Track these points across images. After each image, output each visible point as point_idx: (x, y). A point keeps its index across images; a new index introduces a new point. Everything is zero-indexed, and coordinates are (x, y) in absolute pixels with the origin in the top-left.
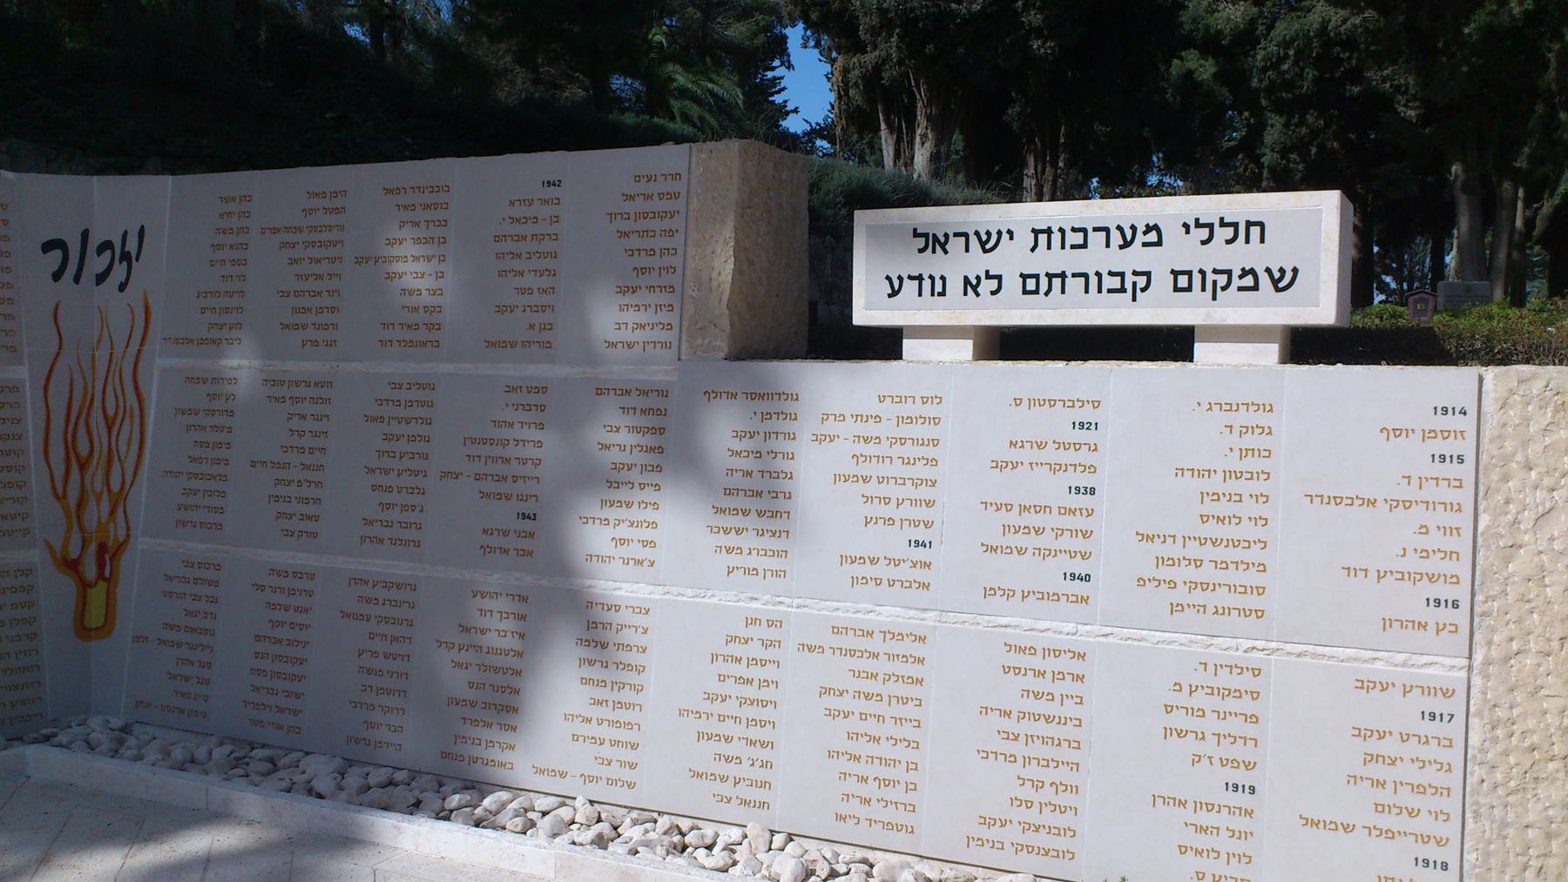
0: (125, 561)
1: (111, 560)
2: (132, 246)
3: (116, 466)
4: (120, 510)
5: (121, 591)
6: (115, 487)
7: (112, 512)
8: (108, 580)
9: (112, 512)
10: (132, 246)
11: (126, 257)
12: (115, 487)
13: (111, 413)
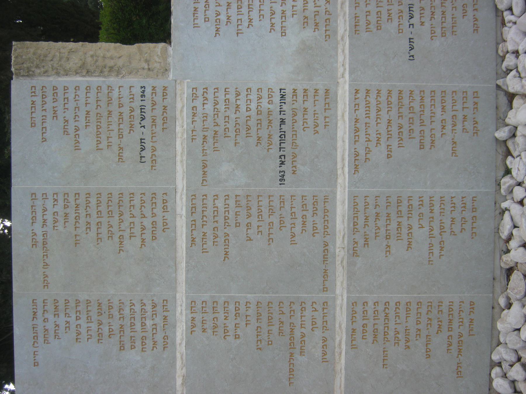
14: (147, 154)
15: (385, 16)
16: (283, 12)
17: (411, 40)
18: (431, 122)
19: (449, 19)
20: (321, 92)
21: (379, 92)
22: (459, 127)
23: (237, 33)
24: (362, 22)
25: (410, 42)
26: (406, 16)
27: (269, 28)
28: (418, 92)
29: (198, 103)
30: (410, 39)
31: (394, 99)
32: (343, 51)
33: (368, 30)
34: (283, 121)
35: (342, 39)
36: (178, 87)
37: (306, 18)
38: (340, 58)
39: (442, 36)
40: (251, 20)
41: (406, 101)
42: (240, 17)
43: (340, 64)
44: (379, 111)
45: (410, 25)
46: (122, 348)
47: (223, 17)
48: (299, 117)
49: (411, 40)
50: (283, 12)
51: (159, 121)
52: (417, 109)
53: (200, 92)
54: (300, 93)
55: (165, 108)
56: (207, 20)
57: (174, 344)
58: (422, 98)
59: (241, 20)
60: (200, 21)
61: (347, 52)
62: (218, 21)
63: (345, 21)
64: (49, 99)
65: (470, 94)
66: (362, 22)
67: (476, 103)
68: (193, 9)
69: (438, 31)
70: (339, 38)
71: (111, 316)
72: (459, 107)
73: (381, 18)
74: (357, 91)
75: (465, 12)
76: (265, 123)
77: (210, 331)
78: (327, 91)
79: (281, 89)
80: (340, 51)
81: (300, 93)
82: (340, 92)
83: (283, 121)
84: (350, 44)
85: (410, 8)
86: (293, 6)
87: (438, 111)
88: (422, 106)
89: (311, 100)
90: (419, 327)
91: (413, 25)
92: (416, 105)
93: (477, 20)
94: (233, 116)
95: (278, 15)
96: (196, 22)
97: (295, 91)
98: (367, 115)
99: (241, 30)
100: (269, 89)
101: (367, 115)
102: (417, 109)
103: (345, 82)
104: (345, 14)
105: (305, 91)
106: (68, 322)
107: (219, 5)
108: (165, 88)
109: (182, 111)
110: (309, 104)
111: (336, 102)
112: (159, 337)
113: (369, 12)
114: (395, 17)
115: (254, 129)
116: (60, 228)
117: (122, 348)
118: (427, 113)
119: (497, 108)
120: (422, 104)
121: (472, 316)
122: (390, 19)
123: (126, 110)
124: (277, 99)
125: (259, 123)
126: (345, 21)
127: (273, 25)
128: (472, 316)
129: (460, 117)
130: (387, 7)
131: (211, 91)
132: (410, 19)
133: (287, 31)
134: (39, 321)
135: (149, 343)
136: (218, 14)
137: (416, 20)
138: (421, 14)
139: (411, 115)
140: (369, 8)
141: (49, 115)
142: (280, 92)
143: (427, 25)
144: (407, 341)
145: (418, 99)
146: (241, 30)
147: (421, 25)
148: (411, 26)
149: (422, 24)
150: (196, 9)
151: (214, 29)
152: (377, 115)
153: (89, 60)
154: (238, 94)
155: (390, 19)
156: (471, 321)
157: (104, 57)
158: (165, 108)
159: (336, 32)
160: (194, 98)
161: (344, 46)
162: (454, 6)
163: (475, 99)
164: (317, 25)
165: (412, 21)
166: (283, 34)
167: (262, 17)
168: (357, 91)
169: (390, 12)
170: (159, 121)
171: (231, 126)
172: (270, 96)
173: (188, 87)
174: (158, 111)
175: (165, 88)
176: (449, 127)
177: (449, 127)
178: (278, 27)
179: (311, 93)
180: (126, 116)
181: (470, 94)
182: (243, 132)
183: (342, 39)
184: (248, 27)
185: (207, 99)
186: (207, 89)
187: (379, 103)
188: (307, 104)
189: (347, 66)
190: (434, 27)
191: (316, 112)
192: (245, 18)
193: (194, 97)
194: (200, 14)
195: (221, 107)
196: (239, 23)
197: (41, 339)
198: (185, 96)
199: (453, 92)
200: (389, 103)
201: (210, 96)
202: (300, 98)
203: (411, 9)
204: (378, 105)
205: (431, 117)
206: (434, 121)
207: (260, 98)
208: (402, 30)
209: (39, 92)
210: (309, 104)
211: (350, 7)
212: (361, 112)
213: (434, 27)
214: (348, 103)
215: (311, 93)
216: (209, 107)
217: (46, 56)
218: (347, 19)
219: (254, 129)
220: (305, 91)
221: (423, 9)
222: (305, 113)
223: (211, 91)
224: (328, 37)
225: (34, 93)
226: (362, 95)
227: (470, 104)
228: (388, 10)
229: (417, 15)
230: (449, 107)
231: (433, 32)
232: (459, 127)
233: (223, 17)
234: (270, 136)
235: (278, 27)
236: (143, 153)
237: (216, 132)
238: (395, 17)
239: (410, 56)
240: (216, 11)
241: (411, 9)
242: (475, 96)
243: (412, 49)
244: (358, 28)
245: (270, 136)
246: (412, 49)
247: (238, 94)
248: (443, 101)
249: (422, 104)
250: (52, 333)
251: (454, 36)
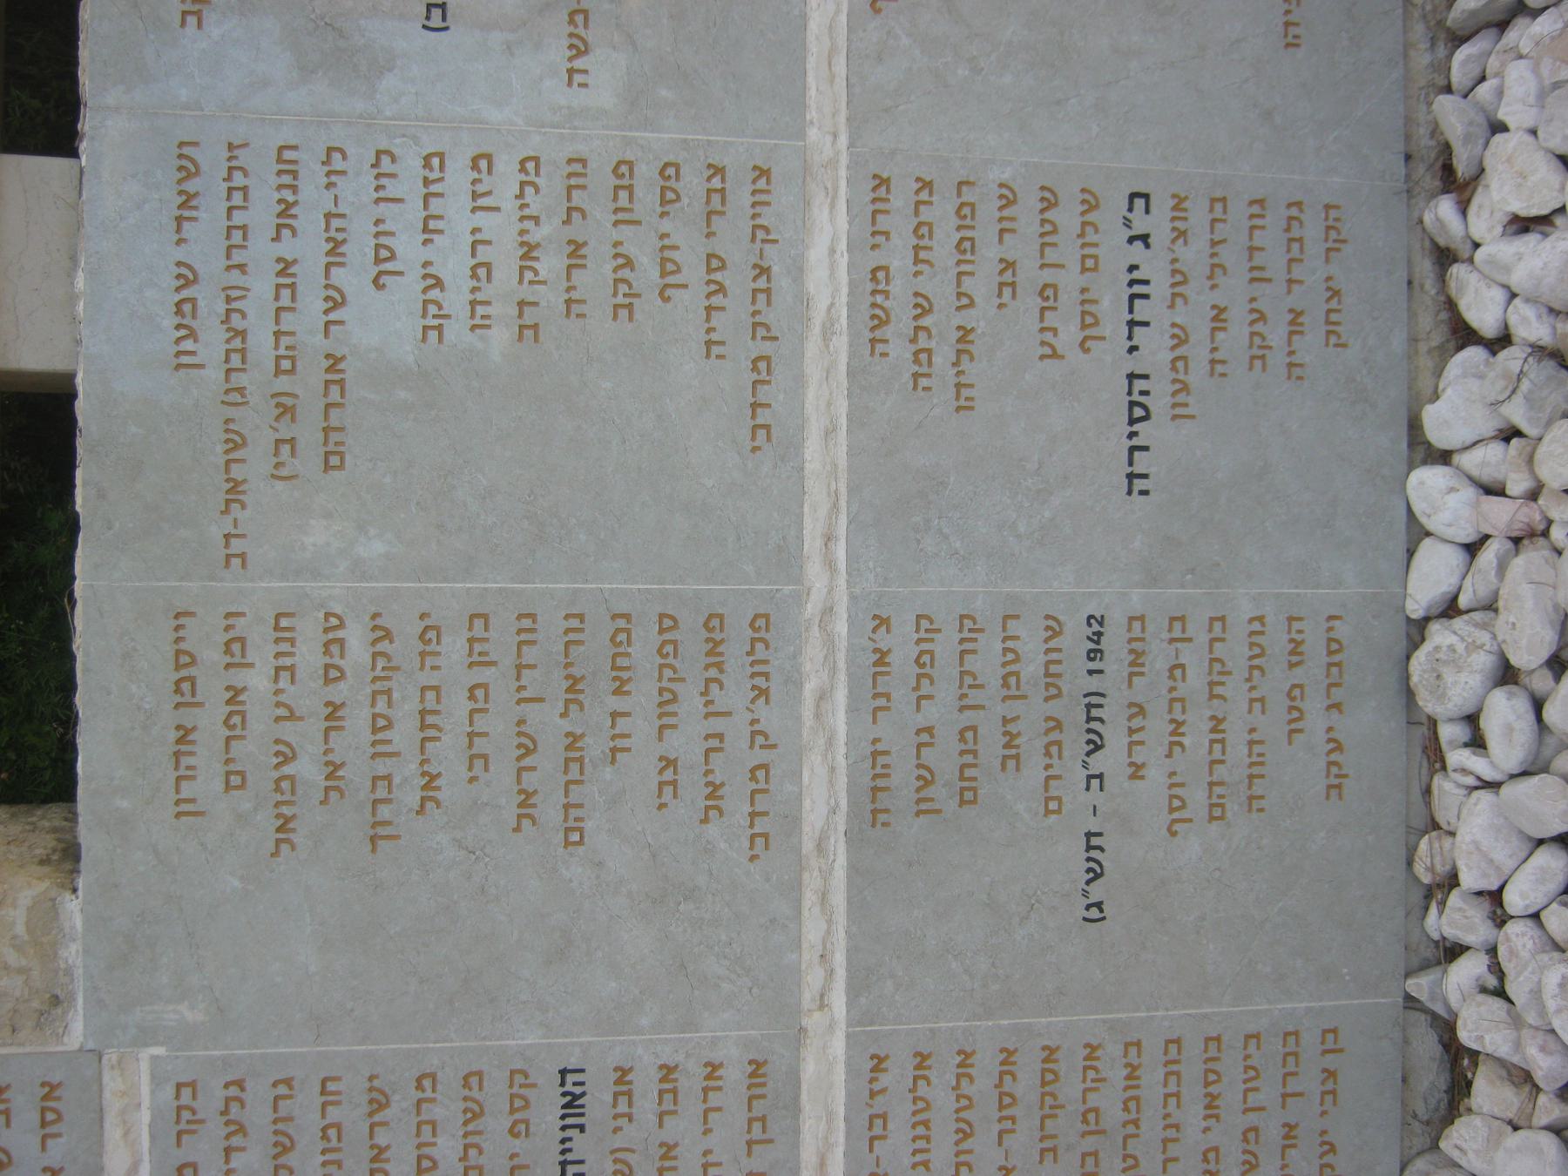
15: (991, 745)
16: (573, 741)
17: (1095, 841)
18: (1166, 1161)
19: (1237, 750)
20: (734, 1075)
21: (966, 1056)
23: (373, 839)
24: (903, 776)
25: (1089, 848)
26: (1075, 742)
27: (510, 814)
28: (1118, 1050)
30: (1089, 835)
31: (1026, 1084)
32: (824, 897)
33: (924, 807)
35: (820, 848)
36: (112, 1082)
37: (669, 763)
38: (813, 930)
39: (1212, 818)
40: (431, 780)
41: (1070, 1088)
42: (382, 768)
43: (809, 956)
44: (965, 1134)
45: (1090, 777)
47: (307, 769)
49: (1095, 841)
50: (573, 741)
52: (1113, 1114)
53: (210, 1102)
54: (646, 1083)
56: (234, 780)
58: (1133, 1073)
59: (388, 778)
60: (207, 784)
61: (839, 899)
62: (285, 786)
63: (833, 769)
65: (1310, 1040)
66: (903, 776)
67: (1330, 1074)
68: (173, 735)
69: (1197, 797)
70: (808, 846)
72: (1267, 1094)
73: (975, 753)
74: (879, 1063)
75: (1296, 714)
78: (757, 1068)
79: (563, 1072)
80: (809, 898)
81: (646, 1083)
82: (809, 1069)
84: (854, 869)
85: (1089, 706)
86: (615, 715)
87: (1192, 1115)
88: (1131, 1102)
89: (691, 1106)
91: (1100, 776)
92: (1109, 1102)
93: (1339, 748)
95: (548, 761)
96: (187, 790)
97: (623, 1074)
98: (918, 1158)
99: (389, 823)
100: (513, 1072)
101: (918, 1158)
102: (1113, 1114)
103: (831, 1027)
104: (830, 742)
105: (668, 1071)
107: (292, 716)
108: (51, 1090)
110: (682, 1128)
111: (794, 1108)
113: (929, 730)
114: (1031, 745)
118: (1152, 1127)
119: (1404, 1080)
120: (1130, 1093)
122: (1012, 757)
126: (833, 769)
127: (527, 799)
129: (1273, 1132)
130: (1001, 709)
131: (259, 1094)
132: (1088, 754)
133: (588, 825)
136: (287, 756)
137: (1110, 760)
138: (1131, 731)
139: (1089, 1143)
140: (931, 713)
142: (563, 1084)
143: (1156, 775)
145: (1118, 1075)
146: (389, 823)
147: (1133, 777)
148: (1095, 783)
150: (185, 735)
151: (266, 822)
152: (957, 1154)
154: (379, 1102)
155: (1012, 757)
159: (793, 821)
160: (183, 1126)
161: (826, 875)
162: (1255, 694)
163: (1329, 1057)
164: (714, 791)
165: (1098, 763)
166: (574, 835)
167: (479, 763)
168: (879, 1063)
169: (1012, 728)
172: (519, 1103)
173: (157, 1081)
175: (51, 1090)
178: (550, 811)
179: (690, 1082)
181: (1310, 1040)
183: (820, 848)
184: (421, 810)
185: (241, 1129)
186: (240, 1084)
187: (965, 1103)
188: (674, 1129)
189: (840, 959)
190: (1182, 785)
191: (711, 1158)
192: (407, 770)
194: (206, 759)
196: (381, 793)
198: (145, 1116)
199: (1248, 1037)
200: (1006, 1100)
201: (258, 1115)
202: (646, 1106)
203: (1095, 712)
204: (962, 1115)
205: (1165, 1141)
206: (1175, 1159)
207: (474, 1113)
208: (1059, 799)
210: (682, 1128)
211: (852, 710)
213: (1182, 785)
214: (841, 1111)
218: (841, 762)
220: (668, 1071)
221: (1141, 711)
222: (667, 1164)
223: (259, 1094)
224: (759, 841)
226: (897, 1077)
227: (1309, 1081)
228: (1005, 721)
229: (1115, 738)
230: (1231, 1094)
231: (1177, 804)
233: (307, 769)
235: (550, 811)
238: (1031, 745)
239: (1088, 907)
240: (277, 741)
241: (1095, 712)
242: (1329, 1045)
243: (1096, 875)
244: (884, 800)
246: (1096, 875)
247: (379, 1102)
248: (1211, 1076)
249: (1130, 1093)
251: (1255, 815)
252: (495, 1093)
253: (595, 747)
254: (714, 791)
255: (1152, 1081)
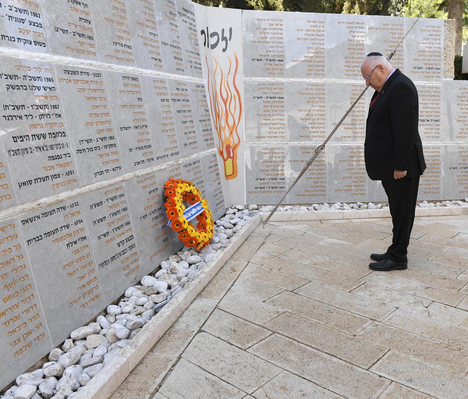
0: (239, 151)
1: (233, 151)
2: (227, 35)
3: (230, 117)
4: (234, 133)
5: (238, 161)
6: (231, 124)
7: (231, 133)
8: (233, 158)
9: (231, 133)
10: (227, 35)
11: (224, 39)
12: (231, 124)
13: (225, 97)
14: (417, 70)
15: (464, 158)
16: (465, 121)
19: (464, 182)
22: (427, 187)
29: (434, 89)
31: (436, 162)
34: (428, 121)
36: (440, 82)
41: (436, 166)
44: (432, 156)
46: (346, 58)
47: (463, 99)
48: (429, 127)
50: (465, 121)
51: (428, 75)
53: (438, 90)
54: (438, 127)
55: (433, 77)
57: (348, 78)
60: (462, 91)
62: (462, 97)
64: (436, 33)
65: (438, 190)
69: (459, 178)
71: (358, 54)
74: (439, 148)
76: (428, 114)
77: (353, 92)
78: (439, 137)
83: (428, 121)
87: (433, 179)
89: (436, 131)
90: (355, 174)
92: (434, 170)
94: (430, 102)
97: (439, 125)
106: (355, 36)
108: (439, 77)
109: (431, 83)
112: (350, 73)
115: (425, 110)
116: (391, 35)
117: (346, 58)
121: (359, 195)
122: (463, 160)
123: (432, 62)
124: (436, 119)
125: (428, 112)
128: (359, 195)
129: (430, 187)
131: (438, 94)
134: (355, 25)
135: (347, 69)
137: (463, 170)
141: (431, 33)
143: (462, 174)
144: (350, 169)
149: (462, 172)
153: (449, 48)
155: (463, 160)
156: (358, 194)
157: (450, 54)
158: (433, 77)
164: (461, 133)
166: (458, 121)
168: (439, 148)
170: (428, 75)
171: (426, 102)
174: (432, 75)
175: (439, 77)
176: (427, 183)
177: (427, 183)
179: (438, 131)
180: (430, 62)
181: (438, 190)
182: (424, 106)
192: (463, 107)
193: (437, 88)
195: (433, 98)
197: (349, 25)
201: (437, 94)
202: (436, 127)
207: (436, 112)
209: (438, 29)
210: (434, 131)
212: (431, 150)
215: (438, 131)
216: (433, 93)
217: (450, 32)
219: (425, 110)
220: (439, 129)
223: (438, 94)
225: (438, 27)
227: (435, 190)
229: (464, 170)
232: (427, 187)
233: (463, 99)
234: (423, 116)
235: (460, 119)
236: (417, 68)
237: (424, 96)
245: (423, 116)
250: (351, 30)
252: (438, 114)
253: (465, 123)
254: (461, 133)
255: (436, 174)
